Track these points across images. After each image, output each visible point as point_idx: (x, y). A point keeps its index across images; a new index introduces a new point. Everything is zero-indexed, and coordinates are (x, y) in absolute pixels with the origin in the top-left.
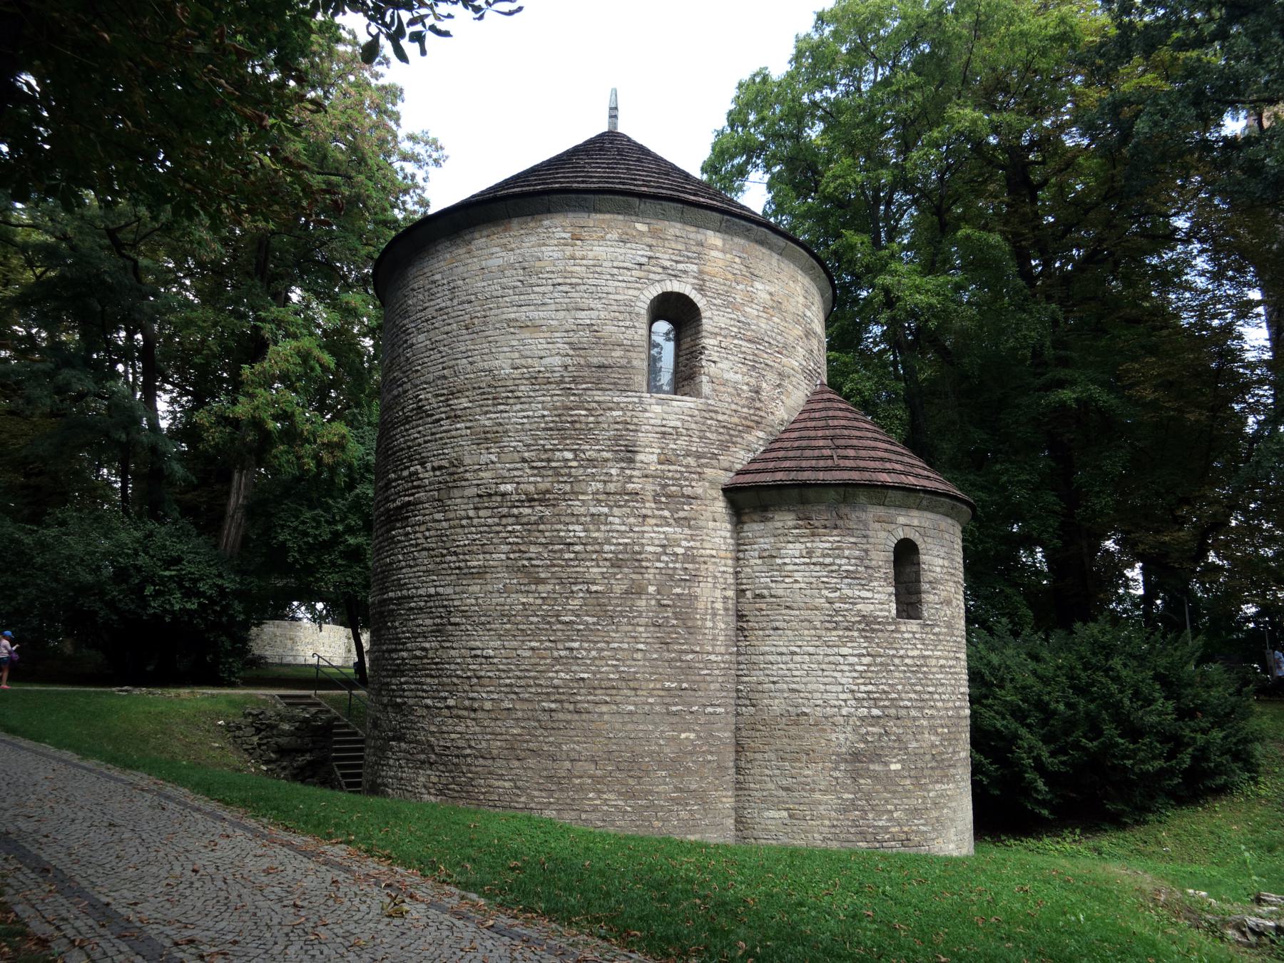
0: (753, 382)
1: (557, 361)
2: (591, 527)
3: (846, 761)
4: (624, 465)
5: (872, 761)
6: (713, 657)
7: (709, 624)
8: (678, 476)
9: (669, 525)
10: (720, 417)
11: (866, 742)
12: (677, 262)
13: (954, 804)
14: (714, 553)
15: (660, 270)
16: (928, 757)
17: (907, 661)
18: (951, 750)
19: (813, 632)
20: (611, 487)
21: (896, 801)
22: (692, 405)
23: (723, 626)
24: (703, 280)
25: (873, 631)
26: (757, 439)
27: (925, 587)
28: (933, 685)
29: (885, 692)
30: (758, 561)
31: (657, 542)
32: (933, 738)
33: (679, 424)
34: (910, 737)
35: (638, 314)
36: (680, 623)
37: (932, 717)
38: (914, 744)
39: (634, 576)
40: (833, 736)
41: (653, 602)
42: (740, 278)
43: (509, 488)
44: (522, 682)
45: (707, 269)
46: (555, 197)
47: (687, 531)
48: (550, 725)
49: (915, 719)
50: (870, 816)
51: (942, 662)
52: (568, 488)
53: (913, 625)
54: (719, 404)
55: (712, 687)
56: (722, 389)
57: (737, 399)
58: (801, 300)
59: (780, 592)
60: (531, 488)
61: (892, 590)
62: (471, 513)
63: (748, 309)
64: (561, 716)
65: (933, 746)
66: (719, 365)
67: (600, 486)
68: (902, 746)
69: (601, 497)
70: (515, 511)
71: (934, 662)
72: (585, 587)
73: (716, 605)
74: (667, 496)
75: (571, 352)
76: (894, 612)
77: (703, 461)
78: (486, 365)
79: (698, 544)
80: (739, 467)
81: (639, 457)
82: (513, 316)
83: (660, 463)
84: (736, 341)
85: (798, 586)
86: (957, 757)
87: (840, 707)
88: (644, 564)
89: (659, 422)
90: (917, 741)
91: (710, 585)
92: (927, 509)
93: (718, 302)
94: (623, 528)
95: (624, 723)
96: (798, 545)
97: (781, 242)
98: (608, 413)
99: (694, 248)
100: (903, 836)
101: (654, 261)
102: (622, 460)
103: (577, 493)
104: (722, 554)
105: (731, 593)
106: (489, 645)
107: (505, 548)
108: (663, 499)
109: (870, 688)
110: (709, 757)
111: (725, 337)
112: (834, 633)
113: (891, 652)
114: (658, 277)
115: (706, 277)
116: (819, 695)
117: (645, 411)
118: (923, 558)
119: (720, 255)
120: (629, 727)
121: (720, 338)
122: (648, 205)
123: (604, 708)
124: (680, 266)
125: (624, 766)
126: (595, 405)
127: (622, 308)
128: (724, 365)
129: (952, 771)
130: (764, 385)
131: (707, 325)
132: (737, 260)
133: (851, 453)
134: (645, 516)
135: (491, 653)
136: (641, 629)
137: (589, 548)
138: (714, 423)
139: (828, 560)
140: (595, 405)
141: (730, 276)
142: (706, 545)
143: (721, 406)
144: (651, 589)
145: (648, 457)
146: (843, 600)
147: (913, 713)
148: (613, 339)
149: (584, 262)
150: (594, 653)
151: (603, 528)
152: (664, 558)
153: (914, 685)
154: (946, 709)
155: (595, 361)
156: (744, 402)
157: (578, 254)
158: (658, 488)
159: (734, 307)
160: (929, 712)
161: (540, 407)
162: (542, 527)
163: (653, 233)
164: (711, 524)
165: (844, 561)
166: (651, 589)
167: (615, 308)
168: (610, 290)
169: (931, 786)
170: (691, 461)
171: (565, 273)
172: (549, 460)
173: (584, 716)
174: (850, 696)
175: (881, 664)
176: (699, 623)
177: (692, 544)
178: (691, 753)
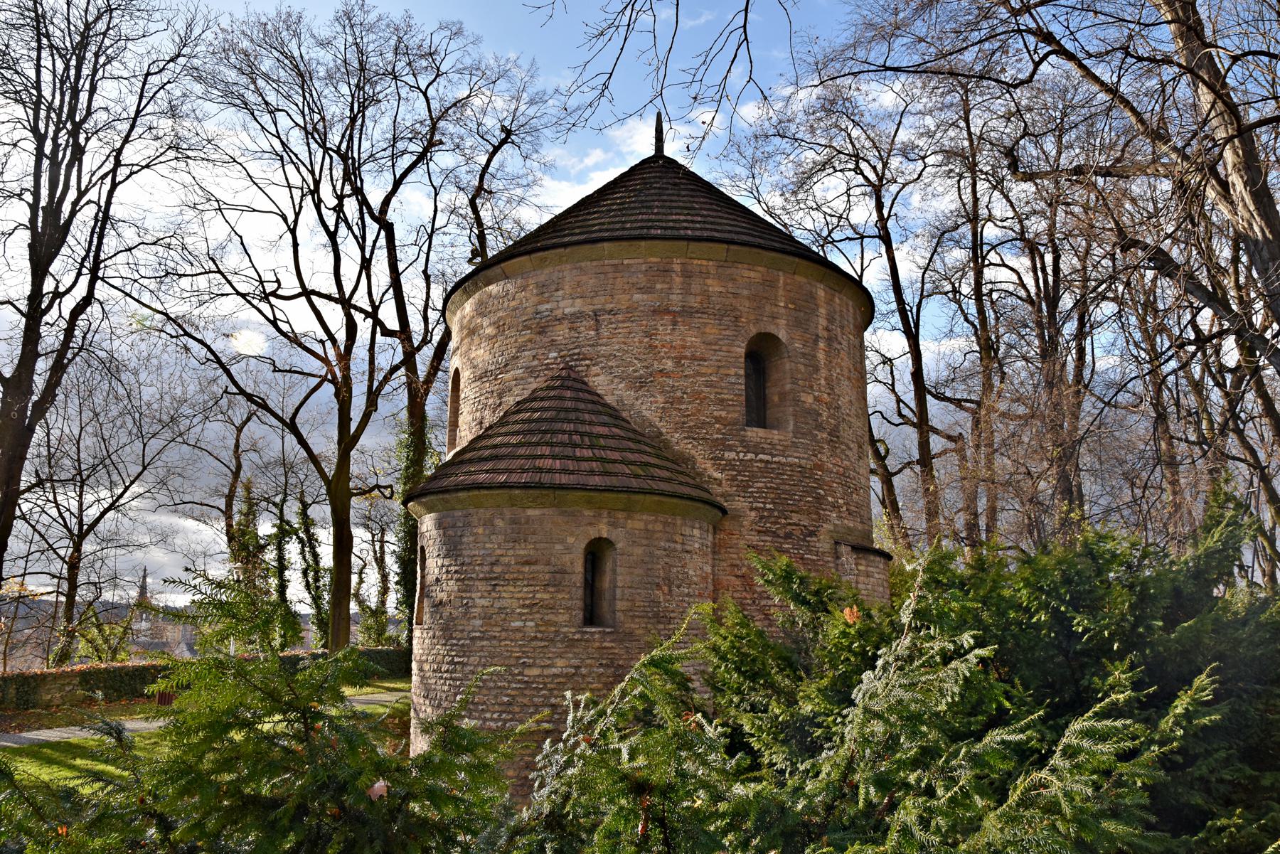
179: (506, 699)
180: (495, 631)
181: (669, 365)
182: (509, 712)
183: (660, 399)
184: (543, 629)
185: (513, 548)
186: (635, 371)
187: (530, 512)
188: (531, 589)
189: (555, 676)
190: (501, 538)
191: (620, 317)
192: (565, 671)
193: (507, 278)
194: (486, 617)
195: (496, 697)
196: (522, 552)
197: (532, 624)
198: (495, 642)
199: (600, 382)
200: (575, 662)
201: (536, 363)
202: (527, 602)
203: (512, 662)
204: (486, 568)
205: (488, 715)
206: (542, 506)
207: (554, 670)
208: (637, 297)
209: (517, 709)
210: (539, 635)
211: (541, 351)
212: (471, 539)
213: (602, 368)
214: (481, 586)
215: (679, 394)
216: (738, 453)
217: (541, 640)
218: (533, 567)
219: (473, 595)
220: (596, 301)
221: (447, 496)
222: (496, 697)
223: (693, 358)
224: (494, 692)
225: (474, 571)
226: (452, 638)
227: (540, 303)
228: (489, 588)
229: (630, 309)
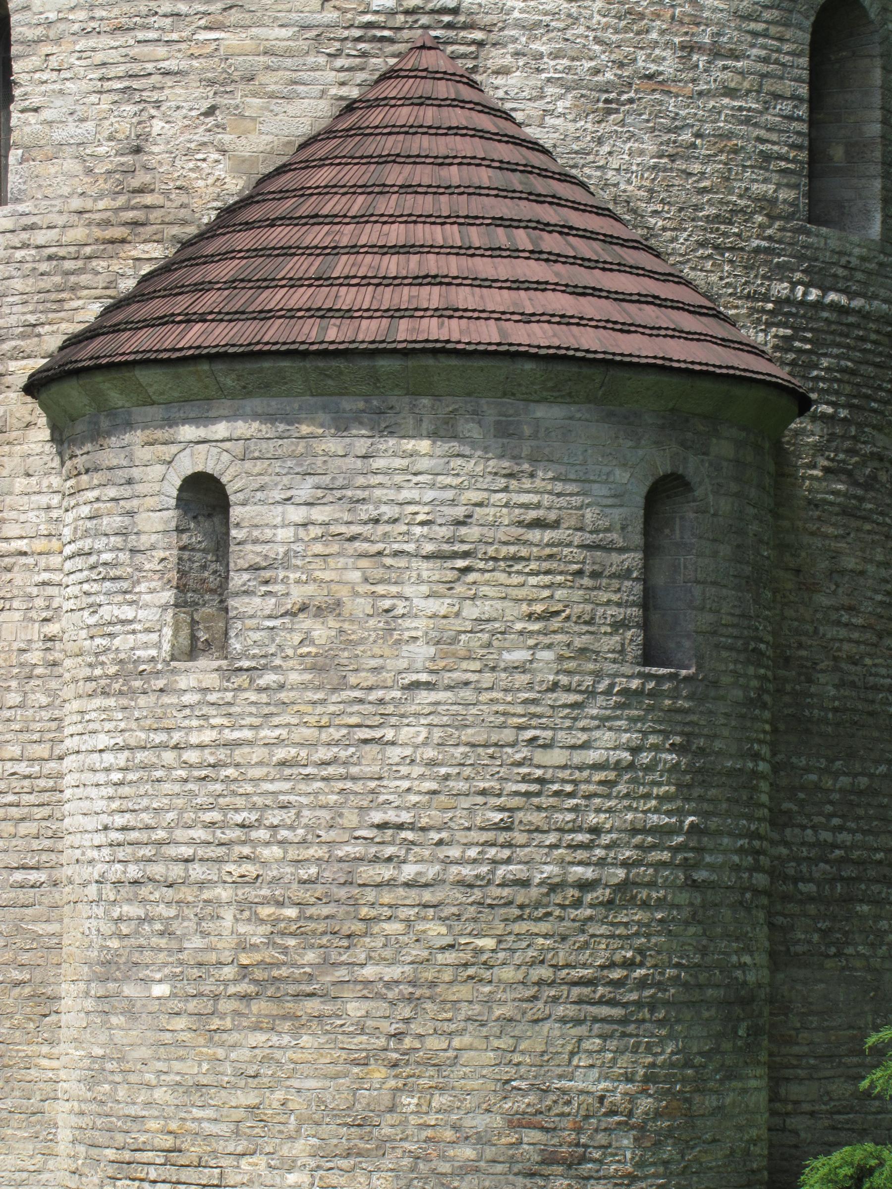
0: (125, 128)
5: (127, 978)
10: (40, 237)
13: (312, 1083)
14: (22, 545)
16: (228, 972)
18: (311, 956)
21: (160, 1066)
23: (44, 700)
27: (237, 580)
28: (254, 807)
29: (148, 828)
32: (242, 929)
34: (191, 925)
37: (243, 881)
38: (197, 942)
49: (202, 885)
50: (121, 1093)
51: (281, 754)
61: (168, 596)
65: (243, 946)
68: (174, 945)
71: (258, 754)
76: (166, 647)
86: (342, 973)
90: (205, 934)
91: (17, 616)
92: (246, 393)
100: (168, 1142)
110: (16, 975)
111: (58, 41)
121: (46, 49)
129: (313, 1006)
147: (197, 871)
153: (202, 808)
164: (20, 484)
169: (235, 1037)
180: (467, 671)
181: (669, 66)
182: (509, 845)
183: (650, 147)
184: (571, 665)
185: (505, 489)
186: (597, 71)
187: (540, 411)
188: (547, 579)
189: (597, 767)
192: (614, 756)
196: (525, 498)
197: (547, 655)
198: (467, 694)
199: (509, 86)
200: (634, 738)
202: (539, 608)
203: (508, 735)
204: (444, 532)
205: (454, 852)
206: (570, 398)
209: (520, 838)
210: (564, 680)
212: (398, 463)
213: (517, 54)
214: (426, 569)
215: (686, 136)
216: (794, 285)
217: (568, 689)
218: (549, 535)
219: (408, 590)
221: (340, 363)
223: (716, 53)
224: (465, 803)
228: (451, 575)
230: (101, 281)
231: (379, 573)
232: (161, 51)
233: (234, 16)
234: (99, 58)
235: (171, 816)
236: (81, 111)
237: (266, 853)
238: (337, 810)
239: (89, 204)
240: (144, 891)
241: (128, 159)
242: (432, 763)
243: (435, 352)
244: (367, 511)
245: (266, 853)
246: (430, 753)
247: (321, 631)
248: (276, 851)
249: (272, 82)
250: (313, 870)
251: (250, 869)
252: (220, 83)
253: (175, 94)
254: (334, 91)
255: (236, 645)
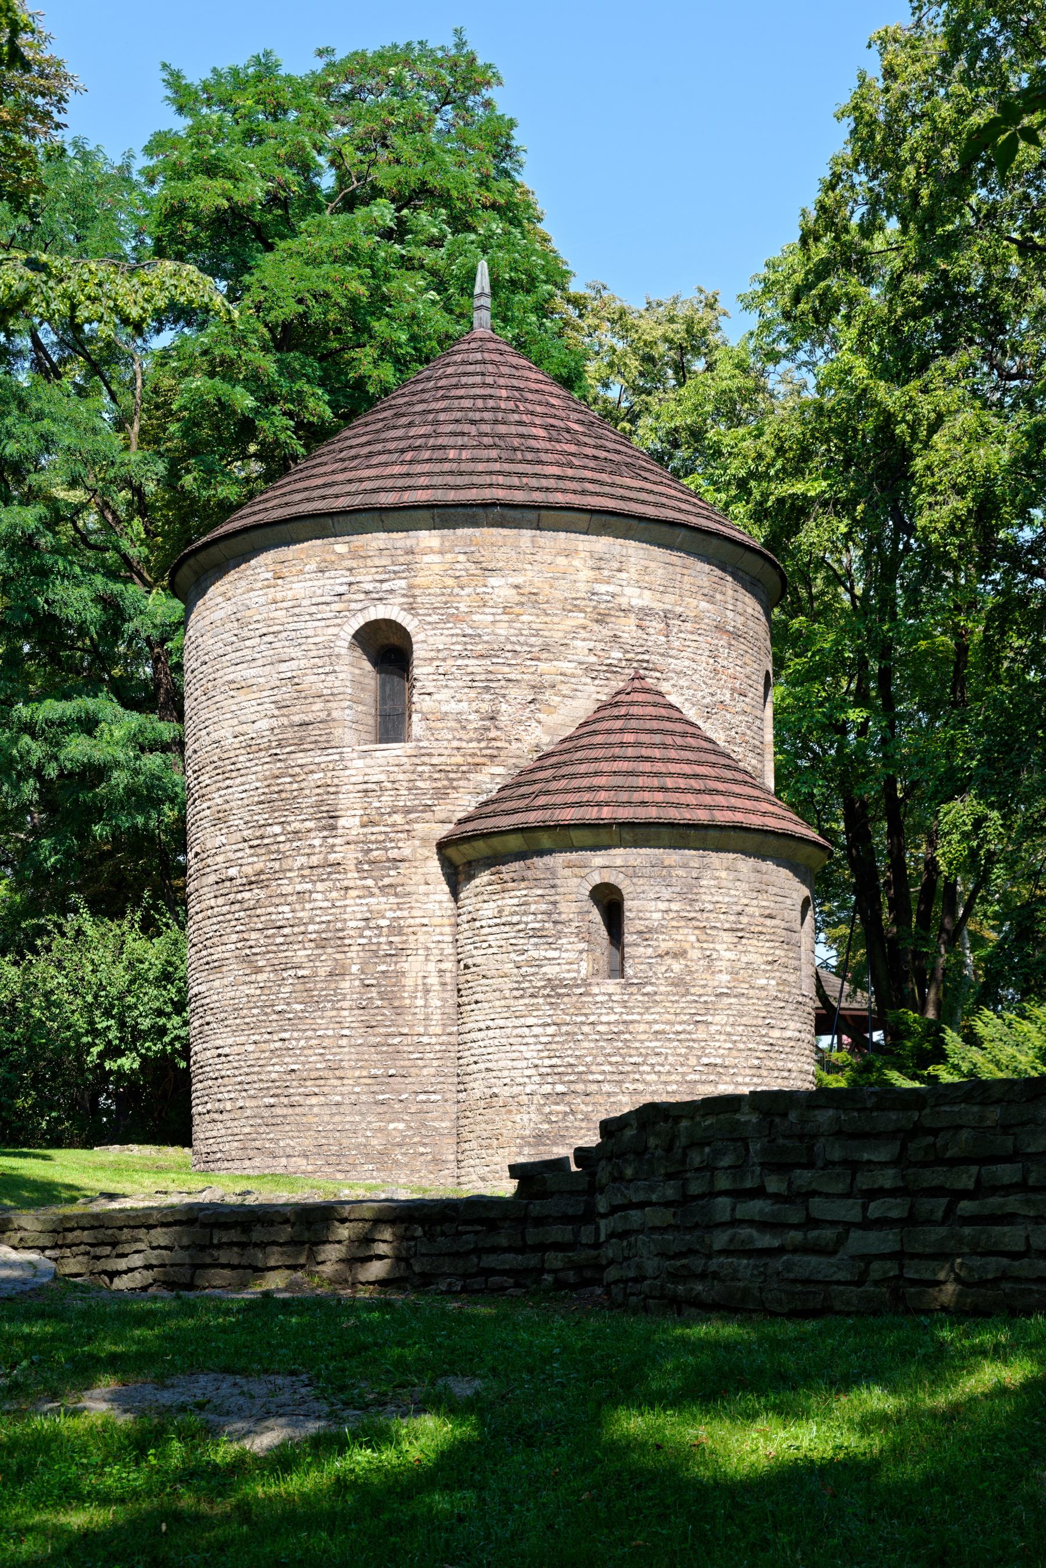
0: (485, 707)
1: (264, 724)
2: (298, 907)
3: (529, 1144)
4: (325, 833)
5: (555, 1144)
6: (425, 1039)
7: (420, 1002)
8: (382, 837)
9: (372, 895)
10: (435, 760)
11: (550, 1122)
12: (382, 581)
14: (425, 921)
15: (362, 596)
17: (600, 1028)
19: (503, 1003)
20: (314, 860)
22: (399, 752)
23: (439, 1003)
24: (414, 596)
25: (559, 995)
26: (491, 779)
30: (466, 926)
31: (359, 916)
33: (383, 777)
35: (338, 656)
36: (385, 1003)
39: (338, 956)
40: (517, 1118)
41: (357, 983)
42: (464, 580)
43: (232, 872)
44: (249, 1079)
45: (417, 581)
46: (254, 535)
47: (393, 900)
48: (271, 1121)
49: (609, 1094)
51: (656, 1027)
52: (277, 865)
53: (612, 986)
54: (435, 744)
55: (425, 1072)
56: (439, 725)
57: (462, 734)
58: (586, 574)
59: (478, 960)
60: (248, 870)
62: (212, 902)
63: (475, 617)
64: (278, 1111)
66: (435, 697)
67: (303, 860)
69: (306, 872)
70: (239, 896)
71: (642, 1027)
72: (292, 972)
73: (428, 981)
74: (371, 862)
75: (276, 712)
76: (583, 972)
77: (412, 816)
78: (215, 736)
79: (405, 913)
80: (461, 815)
81: (341, 822)
82: (231, 677)
83: (363, 826)
84: (460, 662)
85: (490, 951)
87: (524, 1084)
88: (347, 942)
89: (360, 779)
93: (435, 618)
94: (326, 904)
95: (332, 1115)
96: (492, 904)
97: (532, 515)
98: (311, 777)
99: (402, 560)
101: (355, 587)
102: (324, 828)
103: (284, 871)
104: (437, 921)
105: (448, 965)
106: (225, 1040)
107: (234, 937)
108: (366, 867)
109: (554, 1061)
110: (422, 1150)
111: (444, 660)
112: (522, 1001)
113: (579, 1019)
114: (359, 606)
115: (417, 592)
116: (506, 1073)
117: (346, 768)
118: (627, 904)
119: (437, 558)
120: (337, 1119)
122: (342, 522)
123: (314, 1100)
124: (386, 586)
125: (333, 1159)
126: (297, 770)
127: (321, 653)
128: (444, 695)
130: (504, 707)
131: (419, 652)
132: (462, 558)
133: (562, 784)
134: (347, 888)
135: (227, 1051)
136: (345, 1013)
137: (296, 930)
138: (426, 768)
139: (515, 919)
140: (297, 770)
141: (450, 582)
142: (415, 913)
143: (436, 747)
144: (355, 969)
145: (349, 822)
146: (529, 963)
147: (606, 1087)
148: (313, 692)
149: (284, 605)
150: (302, 1043)
151: (308, 906)
152: (367, 933)
154: (666, 1083)
155: (296, 719)
156: (472, 735)
157: (279, 596)
158: (360, 855)
159: (456, 619)
160: (631, 1087)
161: (255, 776)
162: (259, 911)
163: (354, 554)
164: (423, 888)
165: (531, 917)
166: (355, 969)
167: (314, 653)
168: (310, 633)
170: (398, 818)
171: (269, 621)
172: (262, 837)
173: (298, 1110)
174: (533, 1071)
175: (568, 1034)
176: (407, 1002)
177: (399, 914)
178: (399, 1145)
179: (756, 1062)
190: (745, 886)
191: (689, 626)
193: (539, 528)
194: (734, 973)
195: (746, 1059)
197: (773, 982)
198: (743, 1000)
201: (592, 659)
203: (760, 1022)
204: (732, 918)
205: (740, 1079)
207: (788, 1034)
208: (704, 605)
209: (765, 1073)
211: (600, 646)
218: (774, 922)
220: (669, 598)
222: (746, 1059)
225: (718, 920)
226: (687, 993)
227: (596, 581)
229: (698, 619)
230: (471, 784)
231: (703, 937)
232: (506, 669)
233: (544, 655)
234: (470, 670)
235: (589, 1059)
236: (458, 696)
237: (648, 1078)
238: (686, 1056)
239: (464, 744)
240: (567, 1098)
241: (487, 723)
242: (729, 1034)
243: (734, 828)
244: (698, 906)
245: (648, 1078)
246: (728, 1029)
247: (677, 966)
248: (654, 1077)
249: (565, 689)
250: (675, 1087)
251: (640, 1087)
252: (537, 688)
253: (513, 692)
254: (595, 696)
255: (629, 971)
